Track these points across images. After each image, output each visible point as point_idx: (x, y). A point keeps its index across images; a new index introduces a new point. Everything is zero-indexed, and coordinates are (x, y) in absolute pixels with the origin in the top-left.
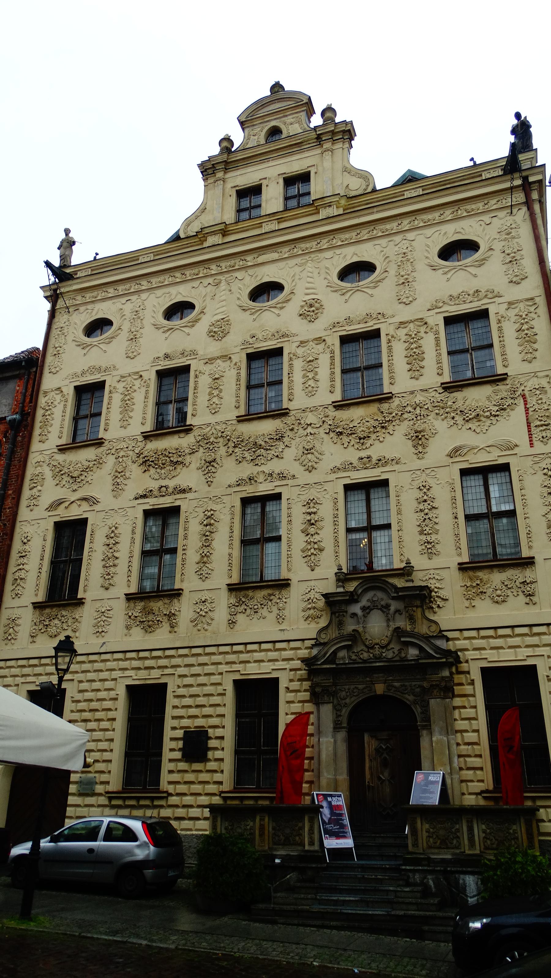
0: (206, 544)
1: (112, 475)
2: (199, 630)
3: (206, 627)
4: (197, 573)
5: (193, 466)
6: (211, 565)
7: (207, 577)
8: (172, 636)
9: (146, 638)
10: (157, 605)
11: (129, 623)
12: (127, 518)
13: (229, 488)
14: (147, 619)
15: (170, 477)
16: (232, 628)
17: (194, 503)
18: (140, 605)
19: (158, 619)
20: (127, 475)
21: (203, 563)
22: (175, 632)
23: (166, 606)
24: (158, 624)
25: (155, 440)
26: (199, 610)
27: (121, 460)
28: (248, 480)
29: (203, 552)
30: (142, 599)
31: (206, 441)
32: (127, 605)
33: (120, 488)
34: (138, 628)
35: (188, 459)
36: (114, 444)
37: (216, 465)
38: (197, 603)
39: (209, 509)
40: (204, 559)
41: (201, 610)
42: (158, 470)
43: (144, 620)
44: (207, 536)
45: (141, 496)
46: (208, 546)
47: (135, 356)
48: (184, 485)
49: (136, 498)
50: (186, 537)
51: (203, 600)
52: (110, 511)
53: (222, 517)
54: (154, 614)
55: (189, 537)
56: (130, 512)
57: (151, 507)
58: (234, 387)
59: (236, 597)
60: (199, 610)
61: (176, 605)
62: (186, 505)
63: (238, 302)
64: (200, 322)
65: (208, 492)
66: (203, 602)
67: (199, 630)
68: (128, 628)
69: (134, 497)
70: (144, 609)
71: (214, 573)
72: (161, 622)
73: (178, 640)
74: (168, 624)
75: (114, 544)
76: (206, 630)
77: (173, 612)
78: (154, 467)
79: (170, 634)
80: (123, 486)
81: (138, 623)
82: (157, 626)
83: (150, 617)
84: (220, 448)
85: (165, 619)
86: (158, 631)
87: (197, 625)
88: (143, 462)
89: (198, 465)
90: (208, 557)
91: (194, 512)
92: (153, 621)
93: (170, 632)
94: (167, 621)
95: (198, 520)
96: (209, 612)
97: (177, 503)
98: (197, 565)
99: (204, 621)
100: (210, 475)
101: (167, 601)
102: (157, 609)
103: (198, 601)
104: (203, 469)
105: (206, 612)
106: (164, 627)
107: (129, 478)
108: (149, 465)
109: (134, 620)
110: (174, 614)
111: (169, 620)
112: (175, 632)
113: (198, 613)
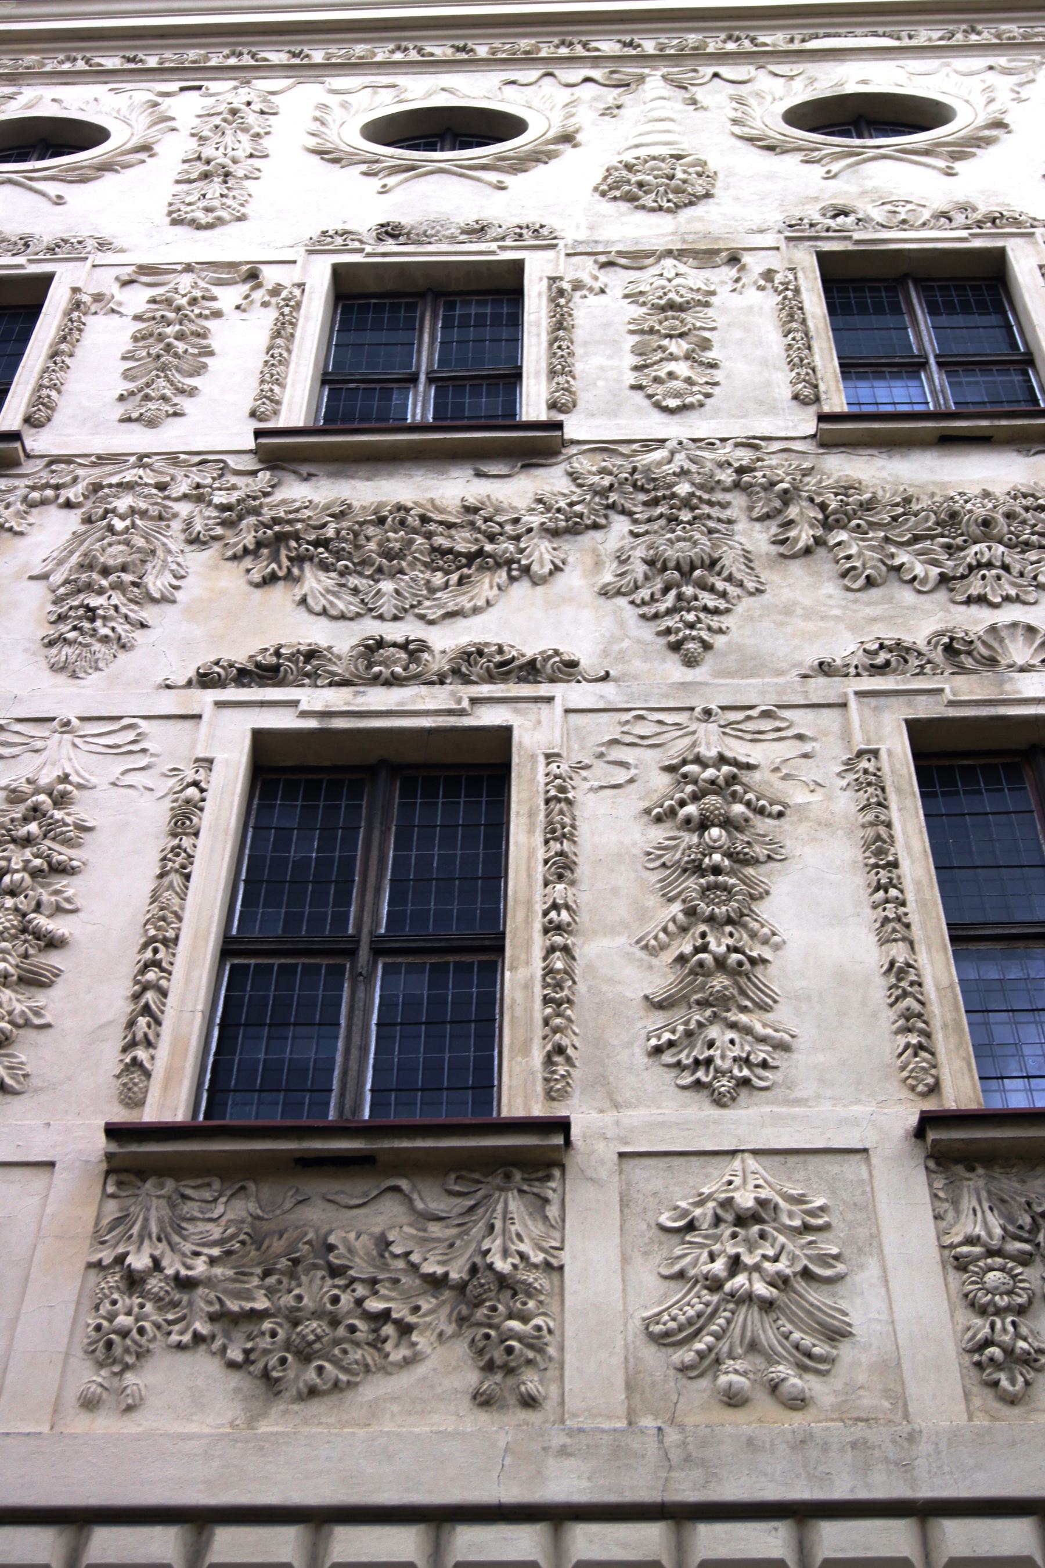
0: (721, 911)
1: (57, 578)
2: (733, 1400)
3: (796, 1382)
4: (668, 1058)
5: (574, 580)
6: (769, 1017)
7: (746, 1082)
8: (504, 1427)
9: (265, 1427)
10: (363, 1223)
11: (123, 1320)
12: (142, 761)
13: (822, 680)
14: (287, 1300)
15: (433, 614)
16: (1012, 1401)
17: (607, 727)
18: (220, 1217)
19: (374, 1305)
20: (156, 583)
21: (703, 1004)
22: (530, 1402)
23: (435, 1229)
24: (377, 1343)
25: (330, 475)
26: (719, 1267)
27: (119, 525)
28: (938, 656)
29: (704, 948)
30: (236, 1174)
31: (642, 497)
32: (112, 1209)
33: (104, 631)
34: (204, 1367)
35: (541, 552)
36: (80, 472)
37: (720, 585)
38: (691, 1227)
39: (712, 753)
40: (717, 980)
41: (735, 1264)
42: (353, 581)
43: (261, 1303)
44: (717, 870)
45: (242, 672)
46: (730, 921)
47: (220, 221)
48: (529, 647)
49: (205, 680)
50: (562, 868)
51: (745, 1200)
52: (18, 727)
53: (798, 796)
54: (335, 1272)
55: (583, 870)
56: (159, 738)
57: (312, 724)
58: (774, 341)
59: (999, 1203)
60: (719, 1267)
61: (513, 1233)
62: (537, 731)
63: (737, 130)
64: (553, 163)
65: (684, 685)
66: (742, 1220)
67: (733, 1400)
68: (113, 1351)
69: (191, 673)
70: (257, 1240)
71: (798, 1066)
72: (405, 1329)
73: (563, 1452)
74: (460, 1349)
75: (36, 874)
76: (798, 1403)
77: (502, 1266)
78: (325, 567)
79: (483, 1418)
80: (122, 628)
81: (202, 1327)
82: (370, 1356)
83: (313, 1290)
84: (738, 527)
85: (435, 1314)
86: (374, 1389)
87: (710, 1363)
88: (259, 544)
89: (607, 577)
90: (736, 972)
91: (600, 767)
92: (335, 1322)
93: (484, 1401)
94: (450, 1329)
95: (632, 802)
96: (800, 1285)
97: (489, 717)
98: (659, 1019)
99: (768, 1336)
100: (691, 617)
101: (432, 1199)
102: (364, 1245)
103: (704, 1213)
104: (644, 593)
105: (782, 1282)
106: (421, 1369)
107: (166, 600)
108: (299, 560)
109: (163, 1304)
110: (503, 1282)
111: (462, 1320)
112: (530, 1402)
113: (715, 1285)
